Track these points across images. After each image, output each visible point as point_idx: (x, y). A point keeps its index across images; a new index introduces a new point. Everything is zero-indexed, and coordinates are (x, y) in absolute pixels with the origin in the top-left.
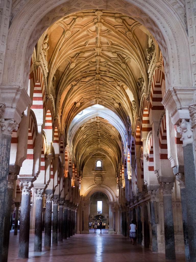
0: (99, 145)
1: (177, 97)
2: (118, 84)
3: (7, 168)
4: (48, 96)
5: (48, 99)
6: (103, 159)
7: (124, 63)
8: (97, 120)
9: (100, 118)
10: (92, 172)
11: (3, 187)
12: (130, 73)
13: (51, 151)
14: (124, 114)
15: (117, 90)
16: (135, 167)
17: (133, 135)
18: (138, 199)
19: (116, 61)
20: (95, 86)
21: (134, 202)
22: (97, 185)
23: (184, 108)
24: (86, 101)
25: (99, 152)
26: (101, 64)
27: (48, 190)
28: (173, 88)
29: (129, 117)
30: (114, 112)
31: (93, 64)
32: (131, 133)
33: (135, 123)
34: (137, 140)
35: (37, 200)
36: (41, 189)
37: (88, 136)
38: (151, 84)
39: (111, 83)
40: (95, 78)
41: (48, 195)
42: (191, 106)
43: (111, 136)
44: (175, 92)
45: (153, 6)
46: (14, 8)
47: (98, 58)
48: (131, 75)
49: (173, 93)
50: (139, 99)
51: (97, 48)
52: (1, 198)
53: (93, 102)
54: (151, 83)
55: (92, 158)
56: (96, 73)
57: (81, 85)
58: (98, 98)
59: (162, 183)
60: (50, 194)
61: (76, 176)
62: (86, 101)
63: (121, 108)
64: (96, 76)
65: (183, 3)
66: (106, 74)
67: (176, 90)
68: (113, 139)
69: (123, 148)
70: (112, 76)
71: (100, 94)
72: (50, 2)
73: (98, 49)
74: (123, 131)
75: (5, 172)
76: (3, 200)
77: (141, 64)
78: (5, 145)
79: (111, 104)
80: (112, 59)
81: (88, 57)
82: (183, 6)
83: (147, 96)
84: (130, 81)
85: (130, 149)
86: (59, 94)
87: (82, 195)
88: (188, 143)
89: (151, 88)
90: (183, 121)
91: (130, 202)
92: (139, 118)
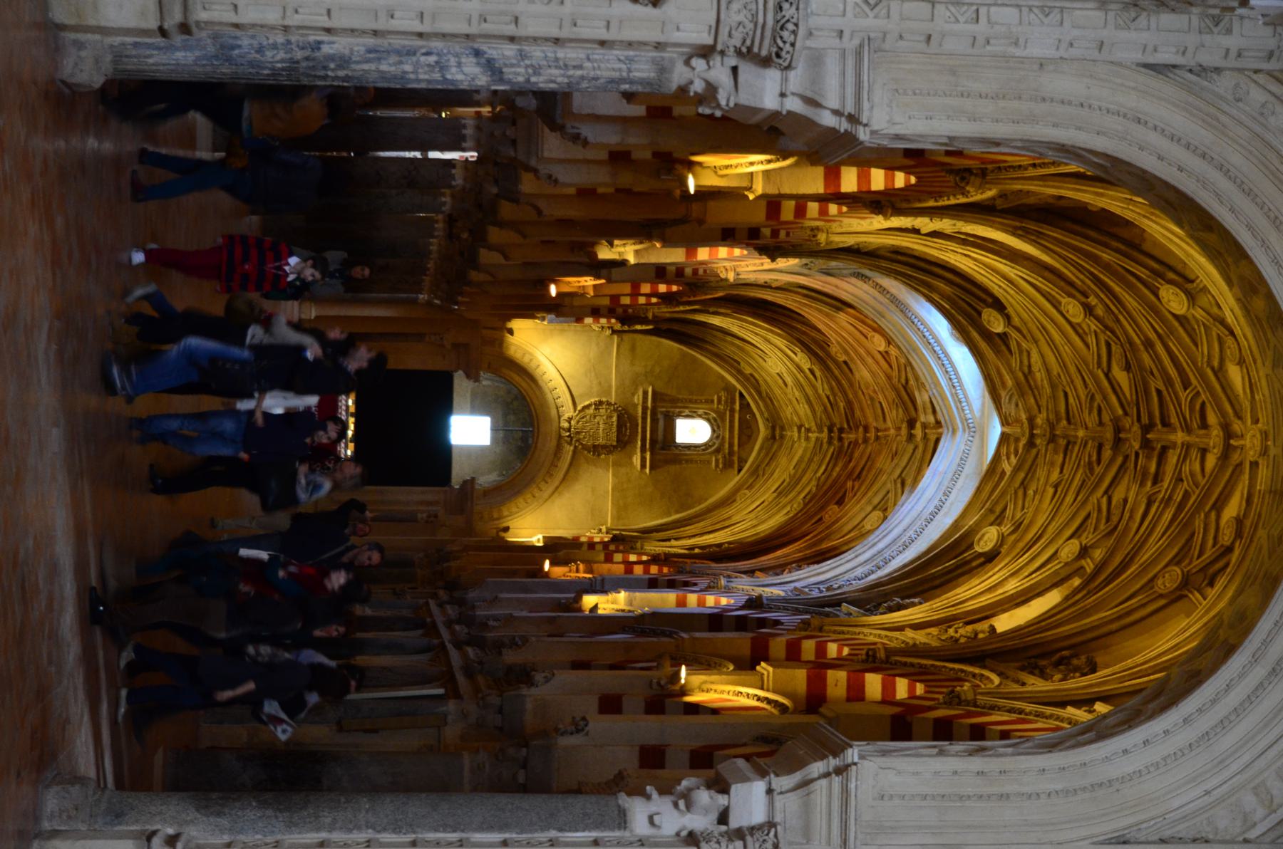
0: (799, 431)
1: (819, 778)
2: (1093, 546)
3: (537, 83)
4: (978, 181)
5: (963, 179)
6: (720, 457)
7: (1186, 583)
8: (924, 426)
9: (937, 441)
10: (645, 393)
11: (464, 74)
12: (1129, 613)
13: (712, 187)
14: (937, 582)
15: (1061, 542)
16: (643, 633)
17: (806, 624)
18: (468, 644)
19: (1198, 539)
20: (1091, 420)
21: (458, 623)
22: (569, 420)
23: (771, 804)
24: (1015, 363)
25: (763, 431)
26: (1194, 453)
28: (855, 764)
29: (921, 603)
30: (956, 525)
31: (1192, 410)
32: (828, 615)
33: (871, 639)
34: (778, 646)
35: (463, 121)
37: (839, 368)
38: (1026, 714)
39: (1100, 510)
40: (1127, 422)
42: (773, 830)
43: (840, 502)
44: (839, 771)
45: (1251, 699)
46: (1249, 77)
47: (1216, 433)
48: (1120, 618)
49: (833, 762)
50: (988, 662)
51: (1258, 436)
52: (420, 70)
53: (1013, 406)
54: (1031, 717)
55: (729, 389)
56: (1147, 429)
57: (1091, 340)
58: (1032, 436)
59: (524, 750)
61: (615, 298)
62: (1015, 363)
63: (974, 564)
64: (1136, 428)
65: (1263, 835)
66: (1142, 484)
67: (845, 774)
68: (820, 519)
69: (760, 570)
70: (1131, 517)
71: (1051, 446)
72: (1273, 237)
73: (1257, 442)
74: (851, 575)
75: (521, 79)
76: (412, 76)
77: (1146, 669)
78: (629, 71)
79: (998, 509)
80: (1213, 515)
81: (1226, 387)
82: (1252, 835)
83: (970, 696)
84: (1086, 613)
85: (742, 608)
86: (1018, 224)
87: (511, 332)
88: (629, 814)
89: (1005, 717)
90: (722, 800)
91: (461, 602)
92: (882, 655)
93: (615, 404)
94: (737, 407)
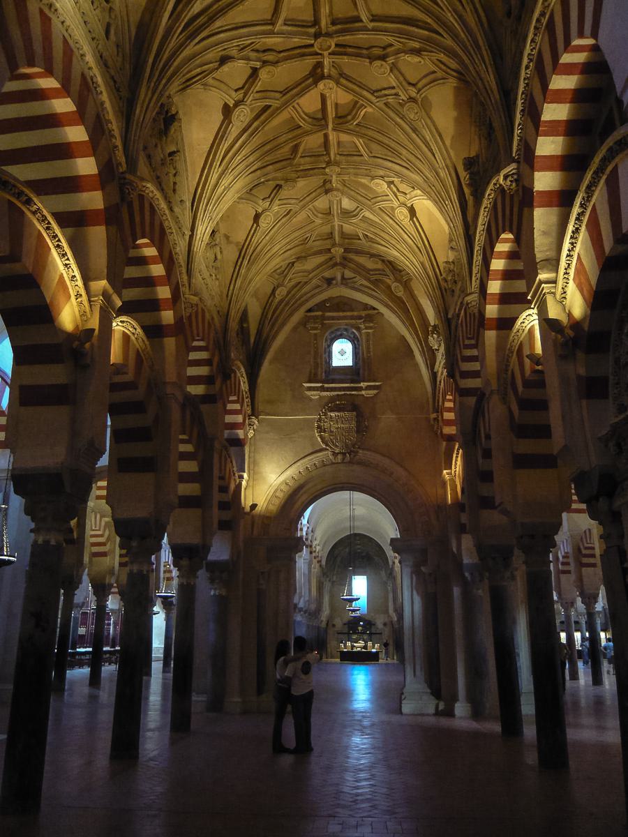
6: (362, 326)
10: (310, 389)
22: (335, 454)
93: (320, 415)
94: (320, 313)
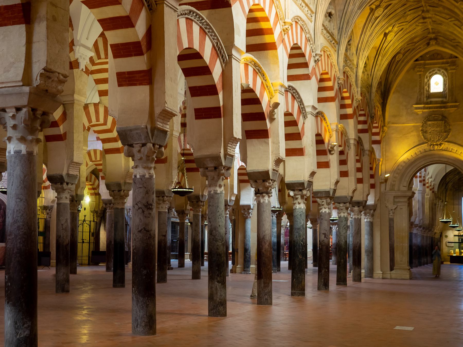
27: (131, 130)
36: (18, 109)
41: (135, 150)
60: (144, 145)
94: (422, 62)
